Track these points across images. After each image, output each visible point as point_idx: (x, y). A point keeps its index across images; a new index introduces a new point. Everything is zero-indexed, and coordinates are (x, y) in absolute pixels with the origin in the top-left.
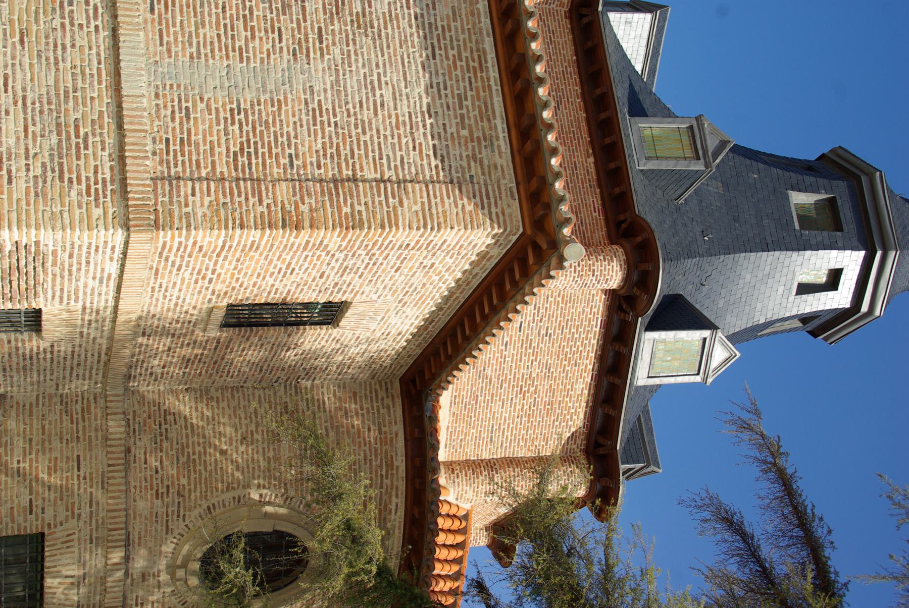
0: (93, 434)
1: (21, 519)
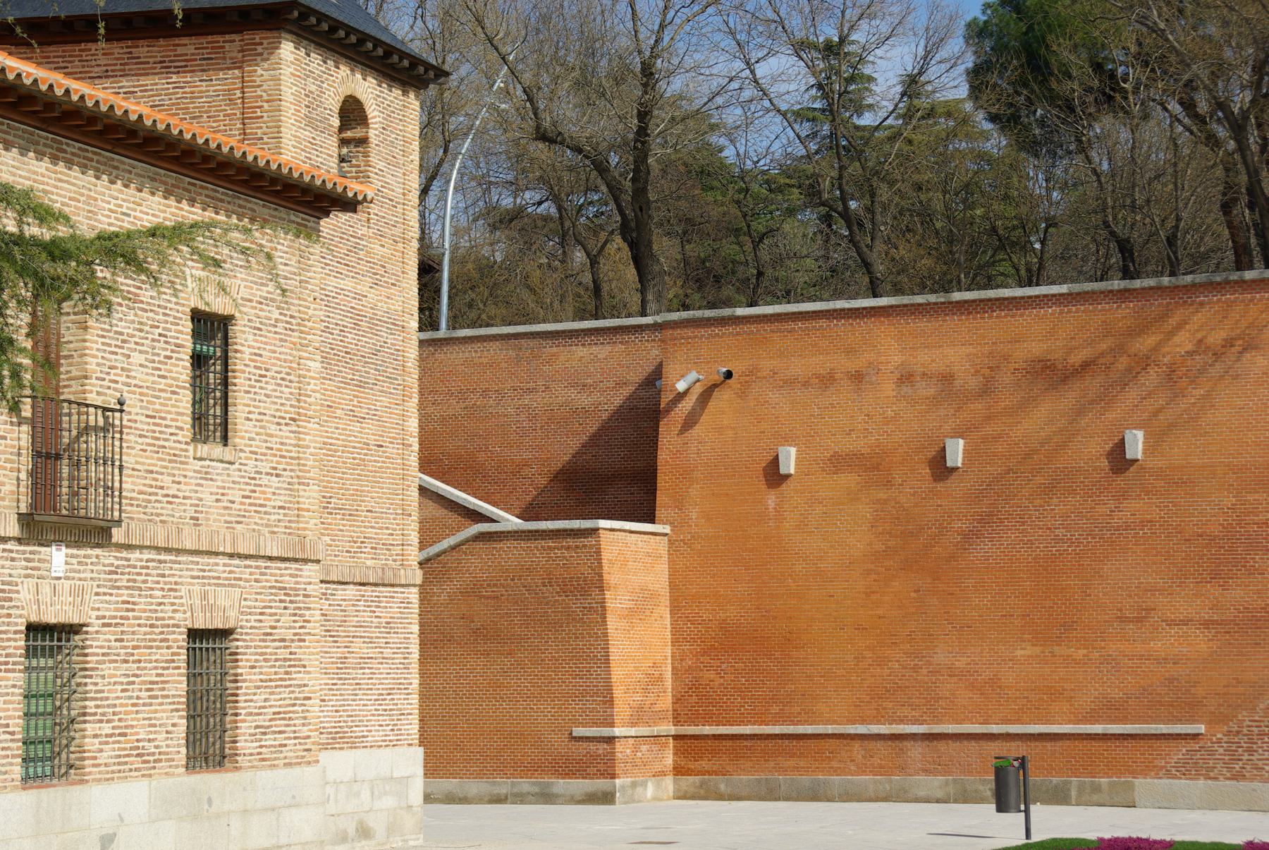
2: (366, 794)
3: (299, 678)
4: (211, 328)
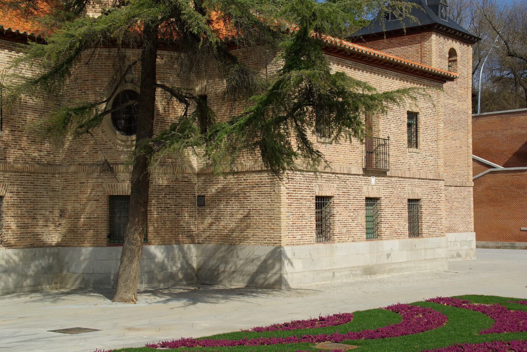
0: (73, 178)
1: (101, 204)
2: (459, 245)
4: (413, 116)
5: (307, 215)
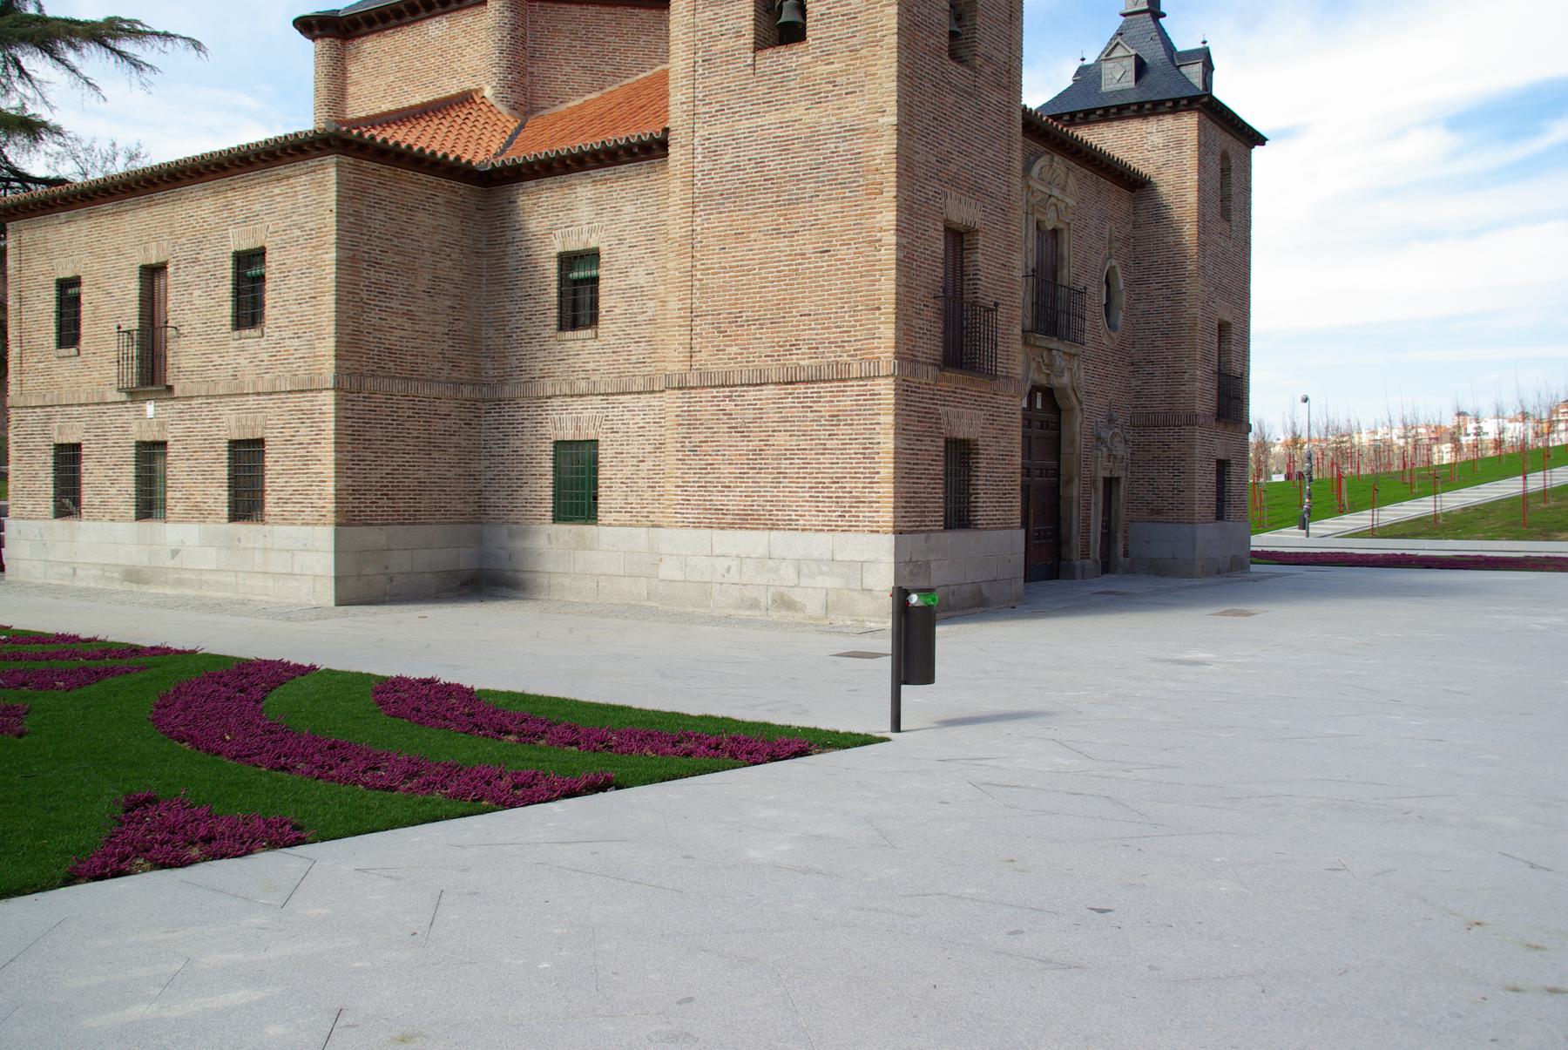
3: (317, 468)
5: (42, 474)
